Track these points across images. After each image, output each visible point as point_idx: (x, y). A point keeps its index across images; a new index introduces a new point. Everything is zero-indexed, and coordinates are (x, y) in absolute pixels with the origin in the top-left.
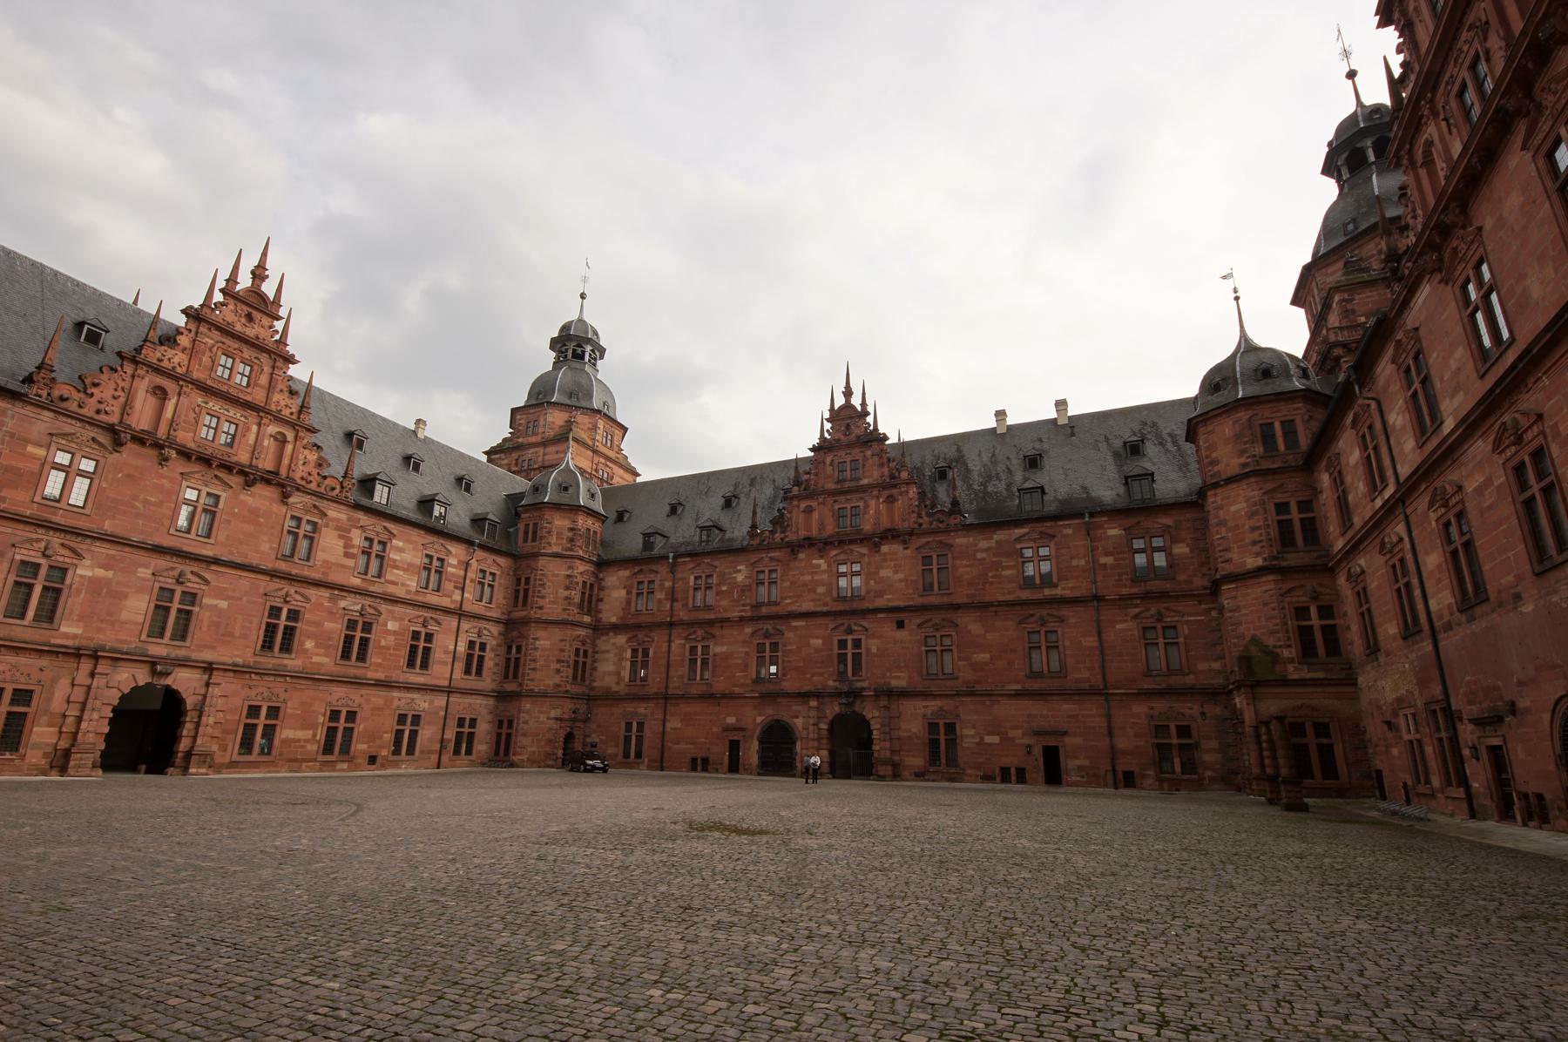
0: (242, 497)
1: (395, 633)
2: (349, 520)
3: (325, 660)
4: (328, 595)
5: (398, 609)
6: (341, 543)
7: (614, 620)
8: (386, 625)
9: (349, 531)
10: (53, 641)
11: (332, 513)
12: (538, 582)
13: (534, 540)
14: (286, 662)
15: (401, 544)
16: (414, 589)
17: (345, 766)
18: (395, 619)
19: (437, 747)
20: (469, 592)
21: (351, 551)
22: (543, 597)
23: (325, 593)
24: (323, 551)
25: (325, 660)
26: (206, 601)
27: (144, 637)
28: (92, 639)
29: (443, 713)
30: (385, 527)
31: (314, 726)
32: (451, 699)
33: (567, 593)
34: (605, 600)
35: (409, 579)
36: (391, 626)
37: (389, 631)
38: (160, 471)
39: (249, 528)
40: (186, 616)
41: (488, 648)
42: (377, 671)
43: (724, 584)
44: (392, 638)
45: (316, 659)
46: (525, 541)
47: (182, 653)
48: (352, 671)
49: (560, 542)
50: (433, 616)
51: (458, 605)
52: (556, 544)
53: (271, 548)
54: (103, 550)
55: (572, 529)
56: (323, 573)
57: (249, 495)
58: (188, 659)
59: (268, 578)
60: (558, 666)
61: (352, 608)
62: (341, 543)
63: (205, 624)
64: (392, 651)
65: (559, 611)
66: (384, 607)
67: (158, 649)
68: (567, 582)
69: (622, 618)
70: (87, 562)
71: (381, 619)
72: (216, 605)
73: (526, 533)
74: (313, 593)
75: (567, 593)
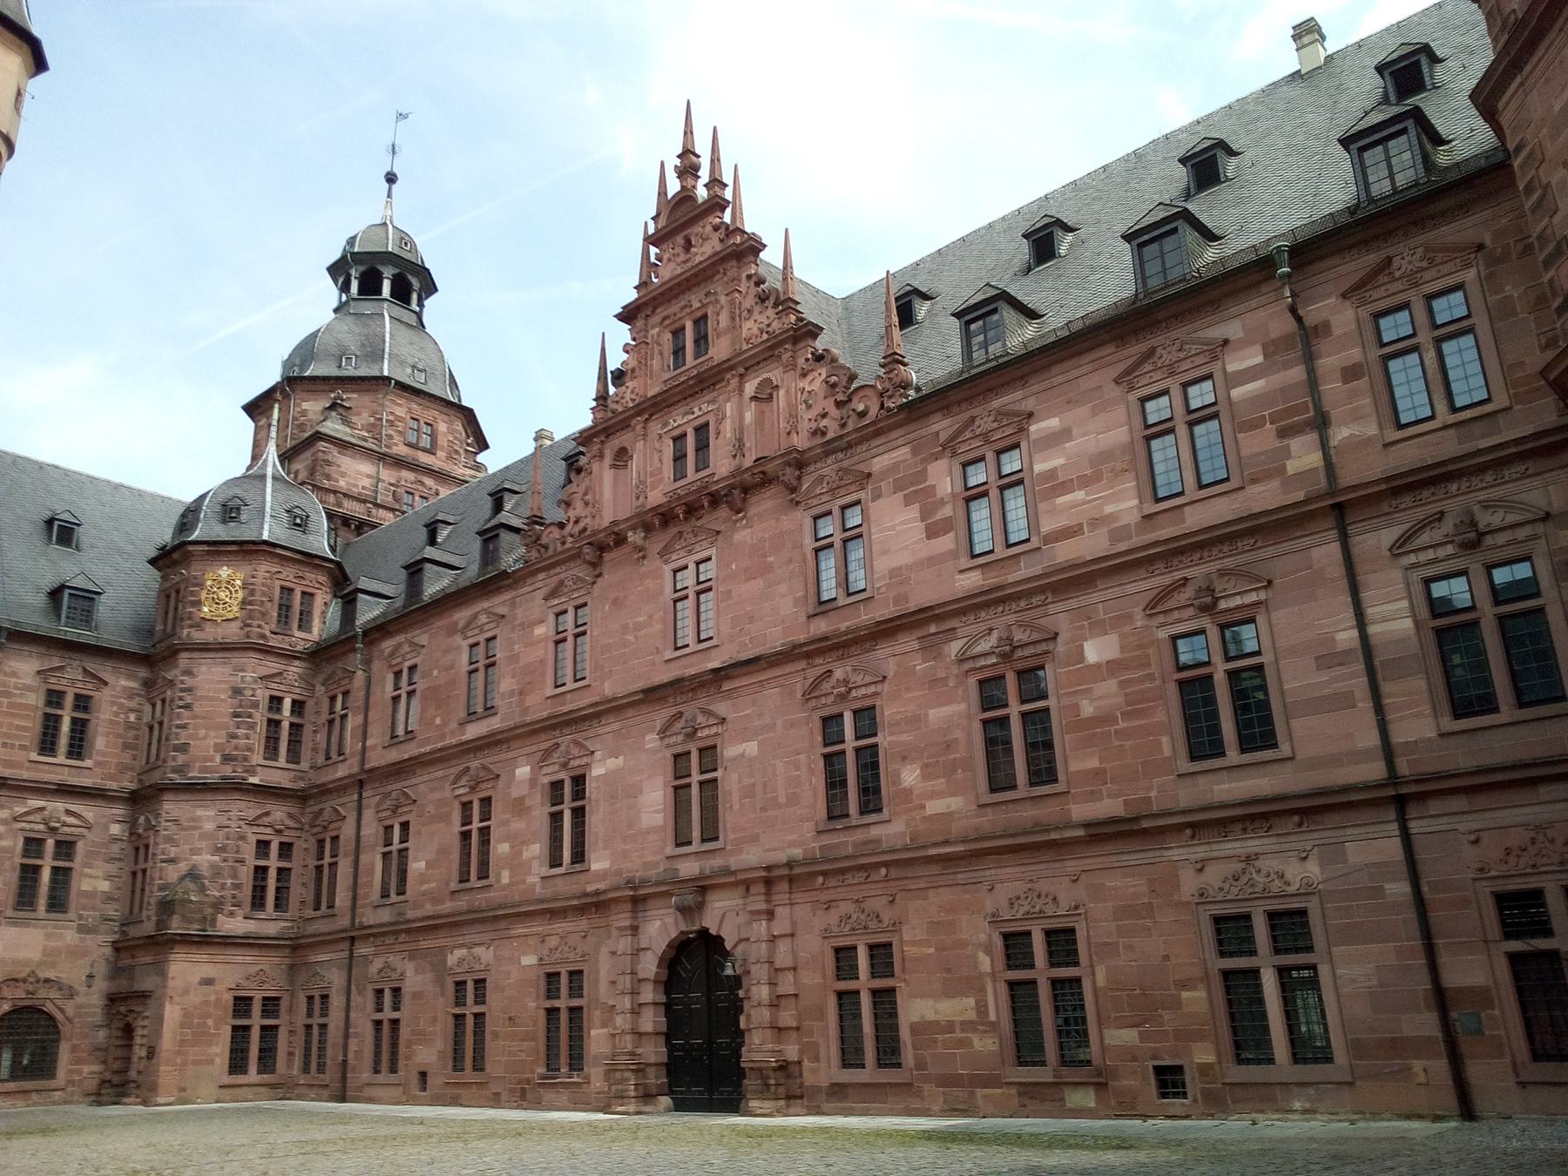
0: (738, 537)
1: (1113, 667)
2: (915, 452)
3: (955, 803)
4: (915, 645)
5: (1098, 598)
6: (914, 511)
8: (1080, 656)
9: (922, 475)
10: (590, 888)
11: (879, 464)
14: (875, 832)
15: (1054, 423)
16: (1133, 518)
17: (1087, 1098)
18: (1099, 628)
19: (1425, 1024)
21: (939, 515)
23: (908, 642)
24: (885, 552)
25: (955, 803)
26: (730, 751)
27: (670, 850)
28: (619, 873)
29: (1400, 889)
30: (1001, 414)
31: (972, 985)
32: (1415, 826)
35: (1107, 500)
36: (1095, 651)
37: (1098, 666)
38: (643, 569)
39: (758, 584)
40: (709, 786)
42: (1094, 796)
44: (1111, 685)
45: (934, 807)
47: (716, 862)
48: (1028, 813)
50: (1229, 563)
51: (1323, 484)
53: (796, 602)
54: (608, 729)
56: (896, 601)
57: (746, 527)
58: (727, 871)
59: (802, 664)
61: (978, 649)
62: (914, 511)
63: (736, 796)
64: (1122, 725)
66: (1059, 615)
67: (689, 868)
70: (598, 755)
71: (1061, 647)
72: (742, 755)
74: (887, 657)
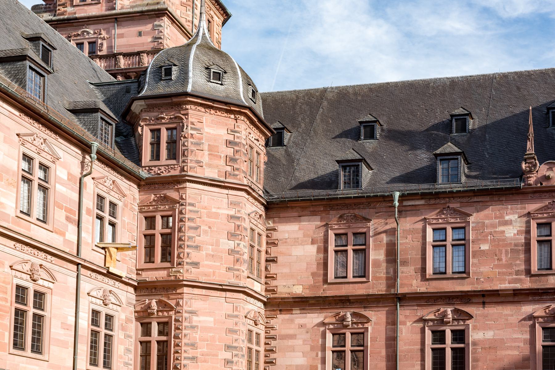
7: (298, 290)
12: (188, 224)
13: (173, 154)
20: (87, 232)
22: (197, 247)
33: (231, 244)
34: (280, 259)
41: (116, 324)
43: (485, 241)
46: (156, 156)
49: (216, 162)
52: (210, 166)
55: (229, 143)
60: (228, 355)
65: (223, 271)
68: (231, 227)
69: (311, 287)
73: (156, 145)
75: (231, 244)
